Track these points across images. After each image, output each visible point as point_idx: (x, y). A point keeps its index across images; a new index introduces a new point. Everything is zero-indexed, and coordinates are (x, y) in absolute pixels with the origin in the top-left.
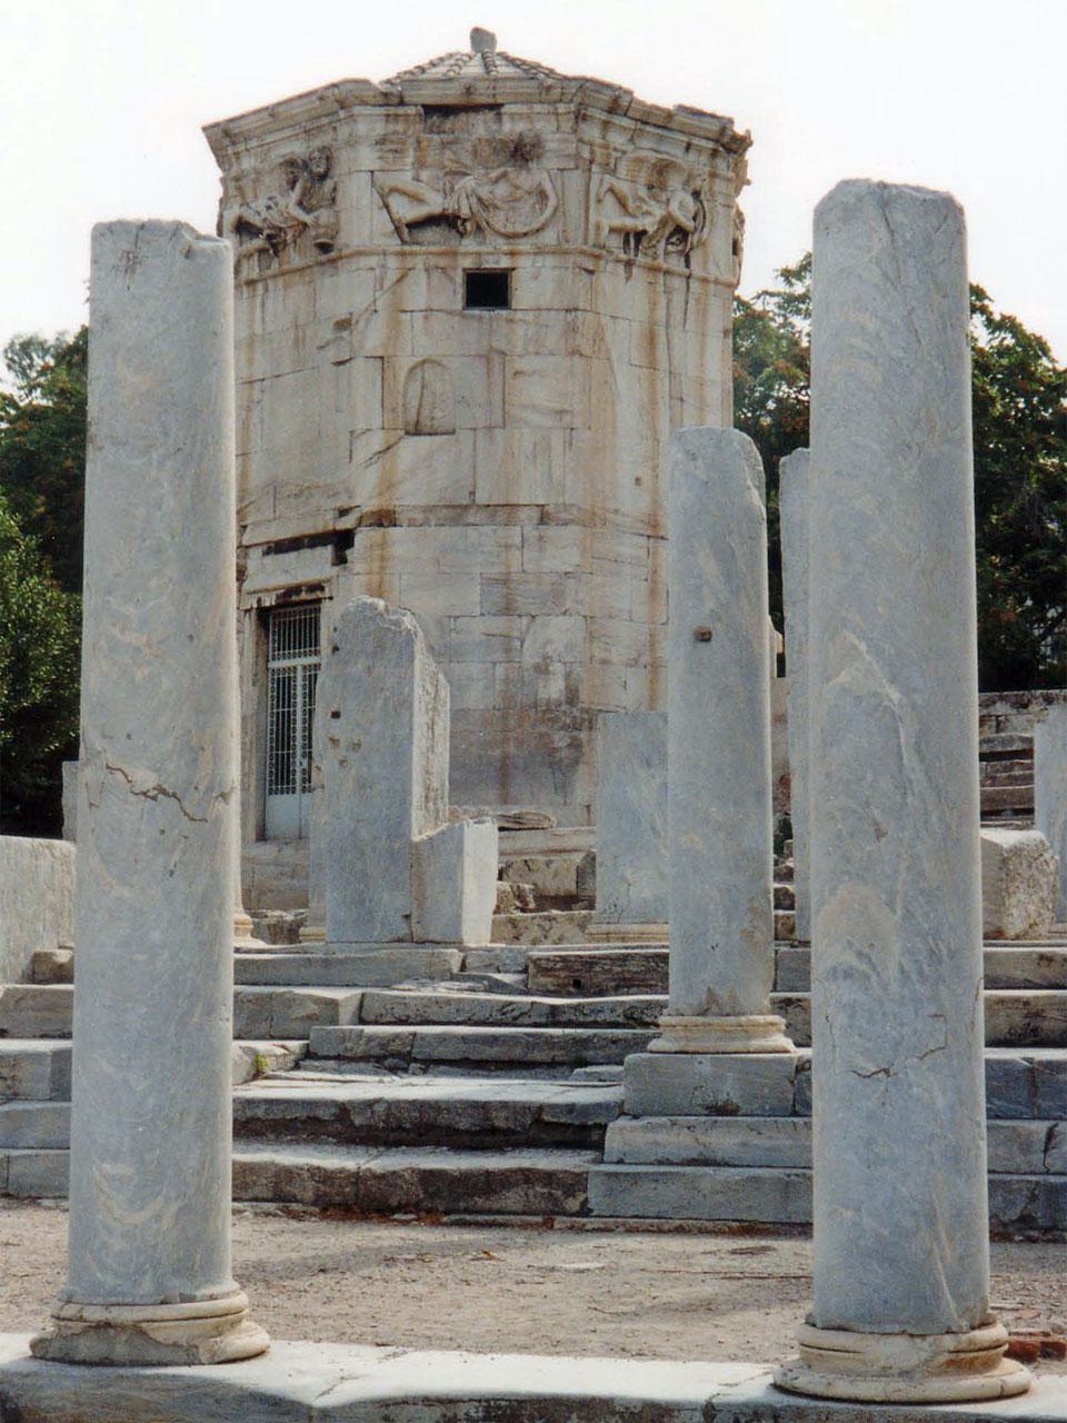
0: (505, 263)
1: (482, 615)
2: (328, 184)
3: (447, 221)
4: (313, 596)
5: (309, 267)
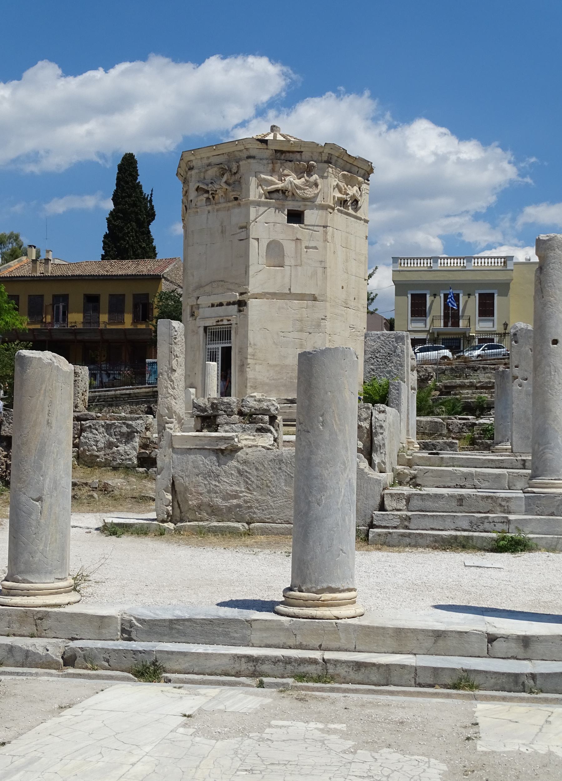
2: (238, 176)
4: (229, 323)
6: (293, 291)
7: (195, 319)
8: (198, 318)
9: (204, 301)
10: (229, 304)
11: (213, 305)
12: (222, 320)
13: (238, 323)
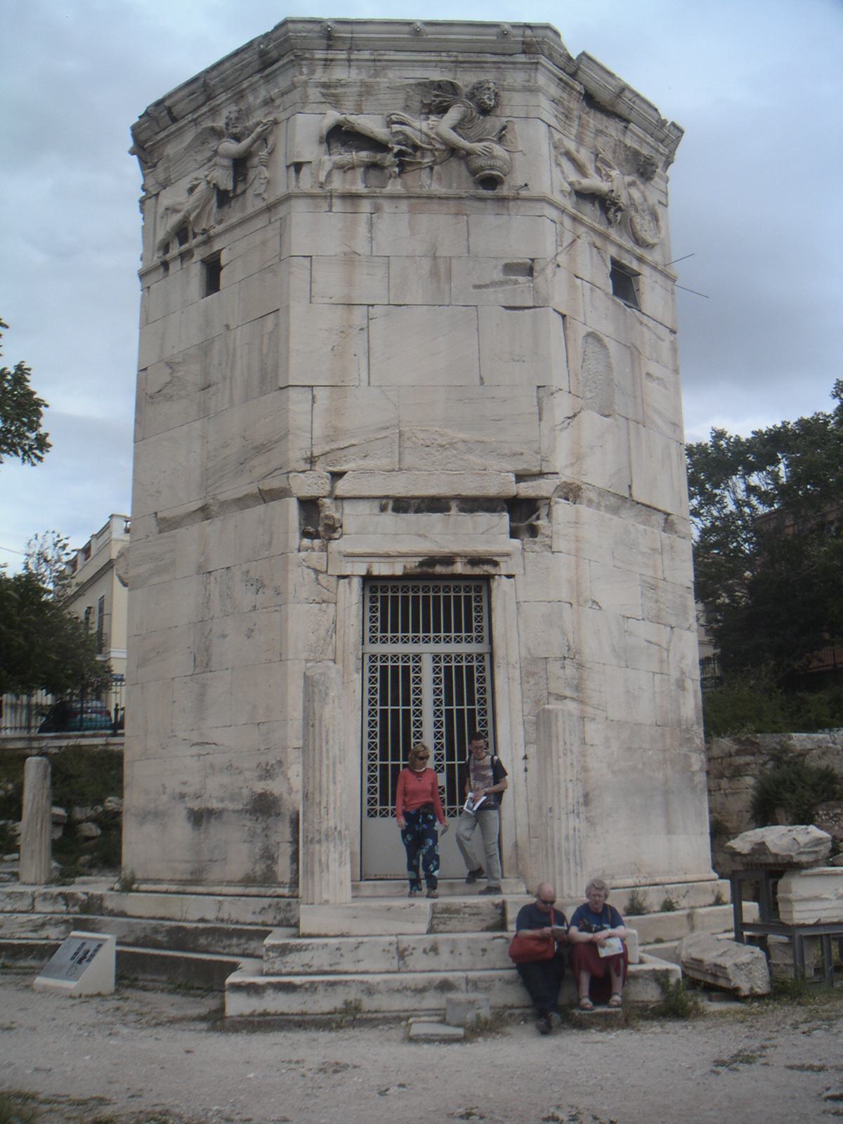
0: (635, 265)
1: (643, 619)
2: (493, 123)
3: (604, 202)
4: (478, 571)
5: (461, 198)
6: (639, 495)
10: (473, 504)
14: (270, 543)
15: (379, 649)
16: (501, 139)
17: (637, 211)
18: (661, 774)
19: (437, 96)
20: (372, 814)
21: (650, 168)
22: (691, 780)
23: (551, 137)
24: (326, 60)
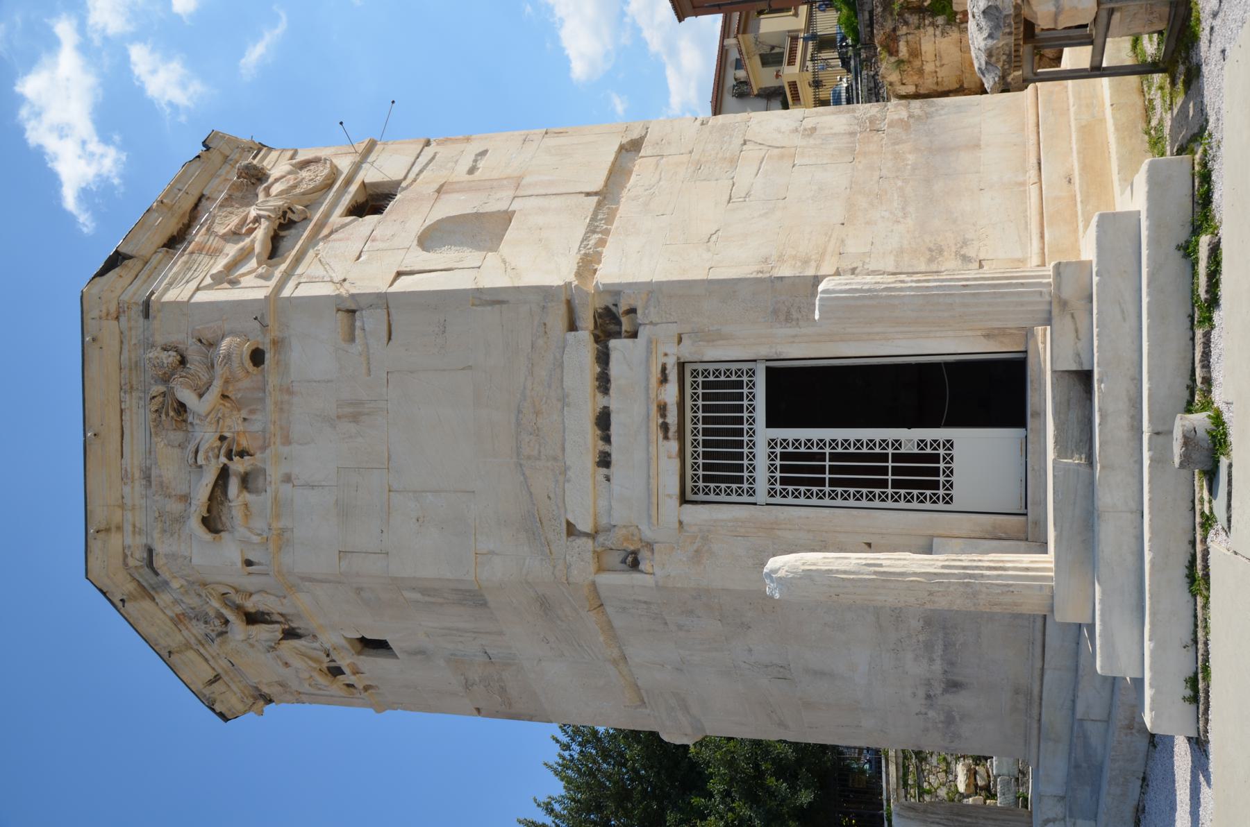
0: (353, 188)
2: (194, 355)
3: (285, 225)
4: (673, 375)
7: (650, 546)
8: (648, 534)
9: (582, 500)
11: (605, 461)
12: (662, 409)
13: (674, 329)
14: (645, 602)
15: (762, 485)
16: (212, 345)
17: (295, 187)
18: (909, 156)
19: (167, 415)
20: (949, 499)
21: (253, 172)
22: (919, 118)
23: (208, 287)
24: (134, 532)
